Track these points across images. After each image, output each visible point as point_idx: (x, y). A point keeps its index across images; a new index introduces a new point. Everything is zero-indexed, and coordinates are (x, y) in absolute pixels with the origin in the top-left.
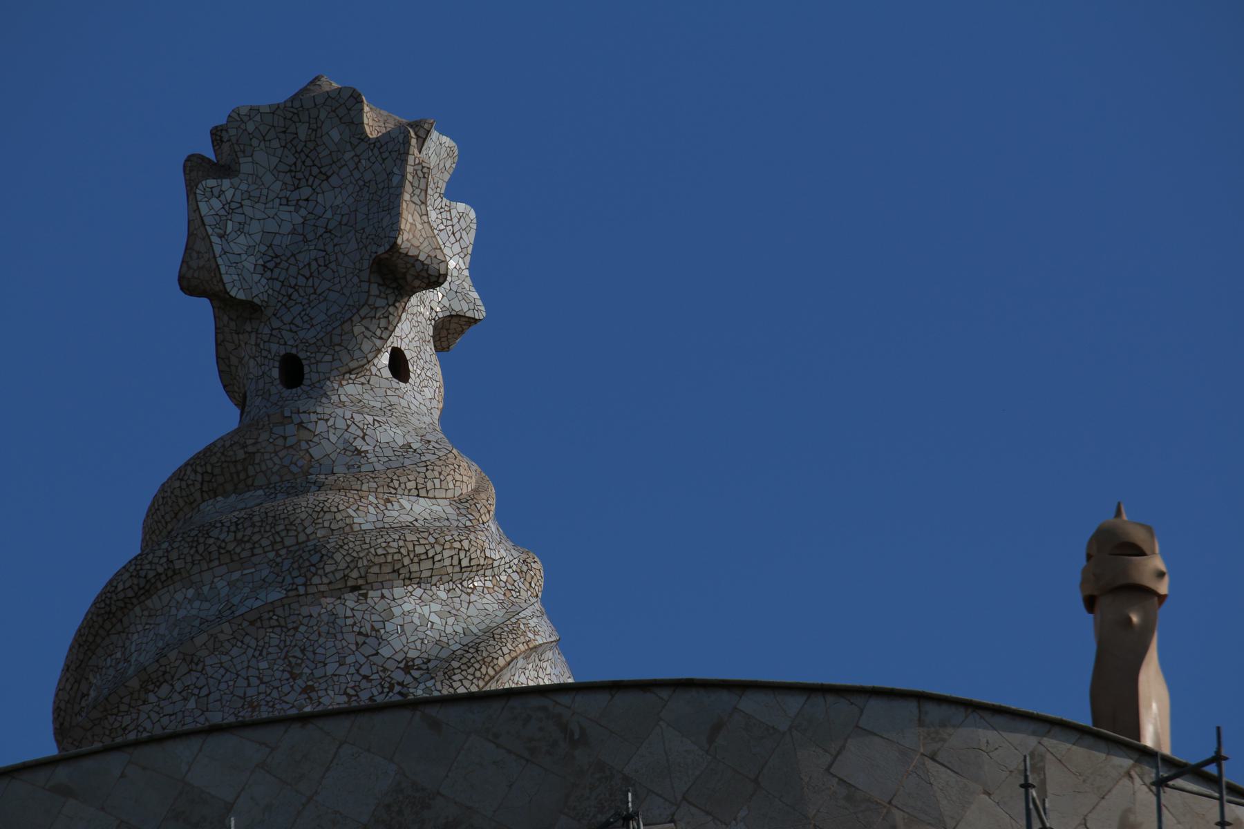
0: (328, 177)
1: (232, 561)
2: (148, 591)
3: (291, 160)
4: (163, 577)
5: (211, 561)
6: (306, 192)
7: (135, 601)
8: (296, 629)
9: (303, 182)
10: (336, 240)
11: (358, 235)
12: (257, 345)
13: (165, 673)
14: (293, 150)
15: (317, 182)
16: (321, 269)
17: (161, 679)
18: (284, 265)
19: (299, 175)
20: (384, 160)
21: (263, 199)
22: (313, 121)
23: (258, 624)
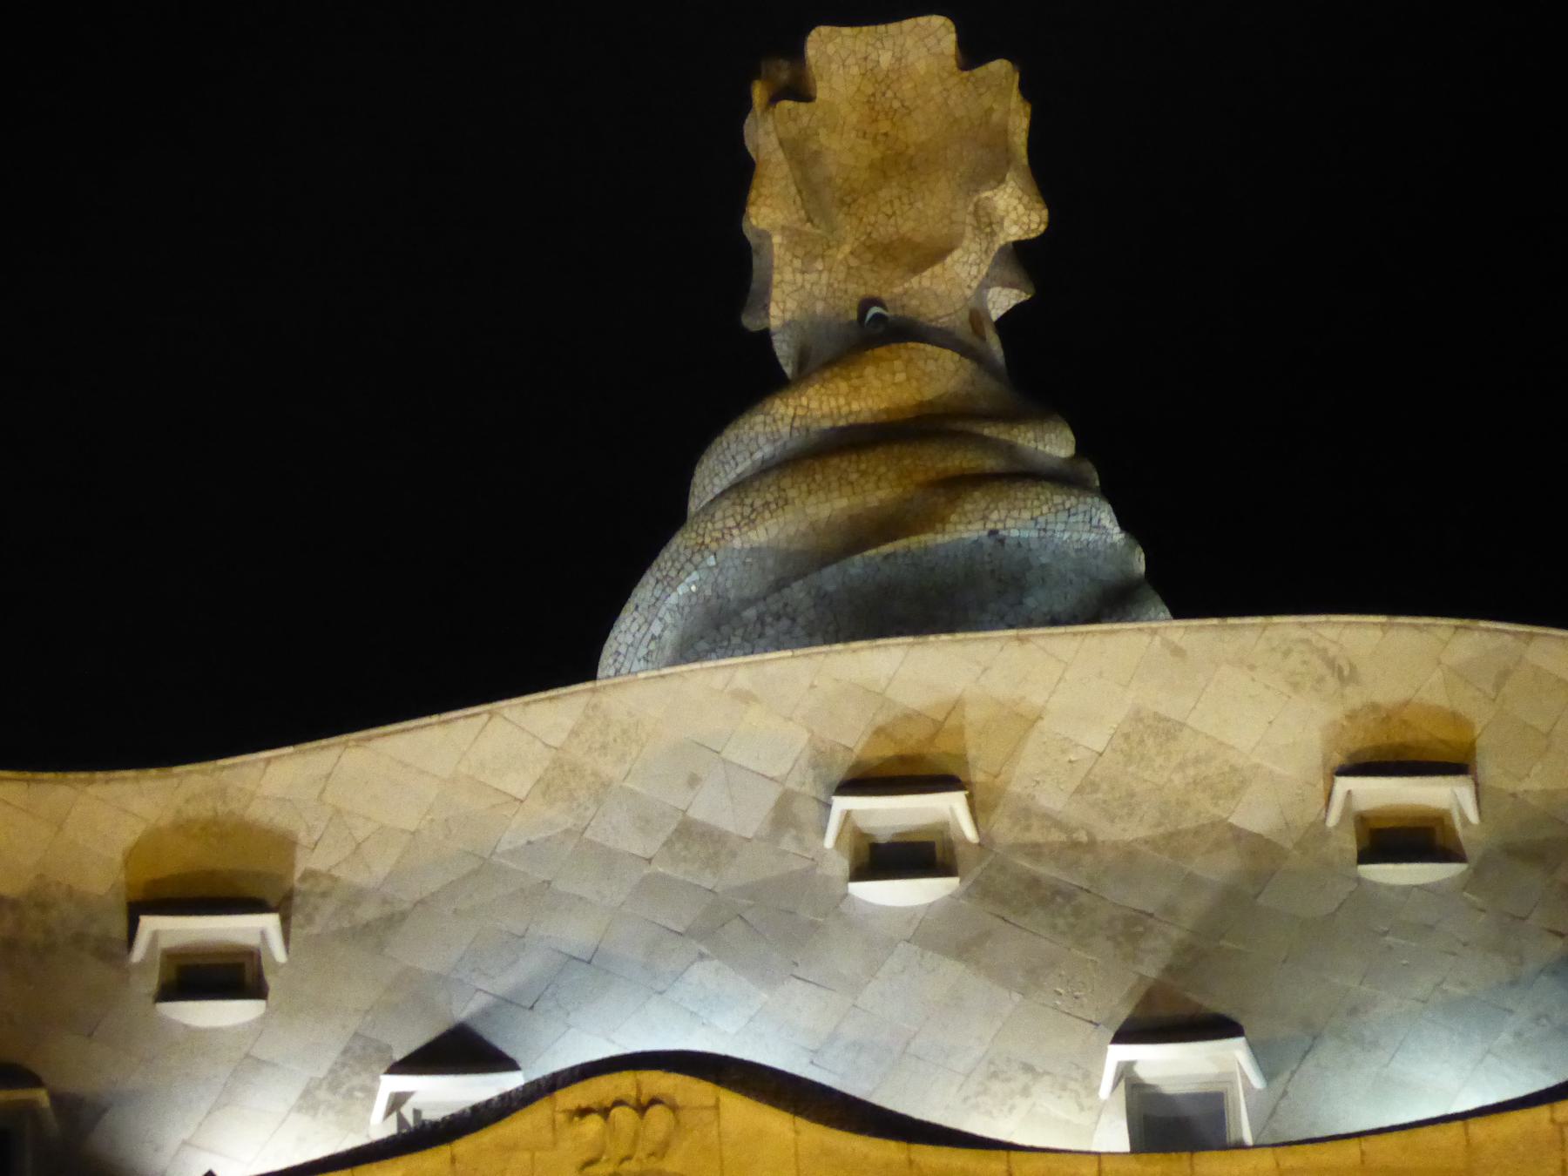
6: (884, 126)
18: (862, 201)
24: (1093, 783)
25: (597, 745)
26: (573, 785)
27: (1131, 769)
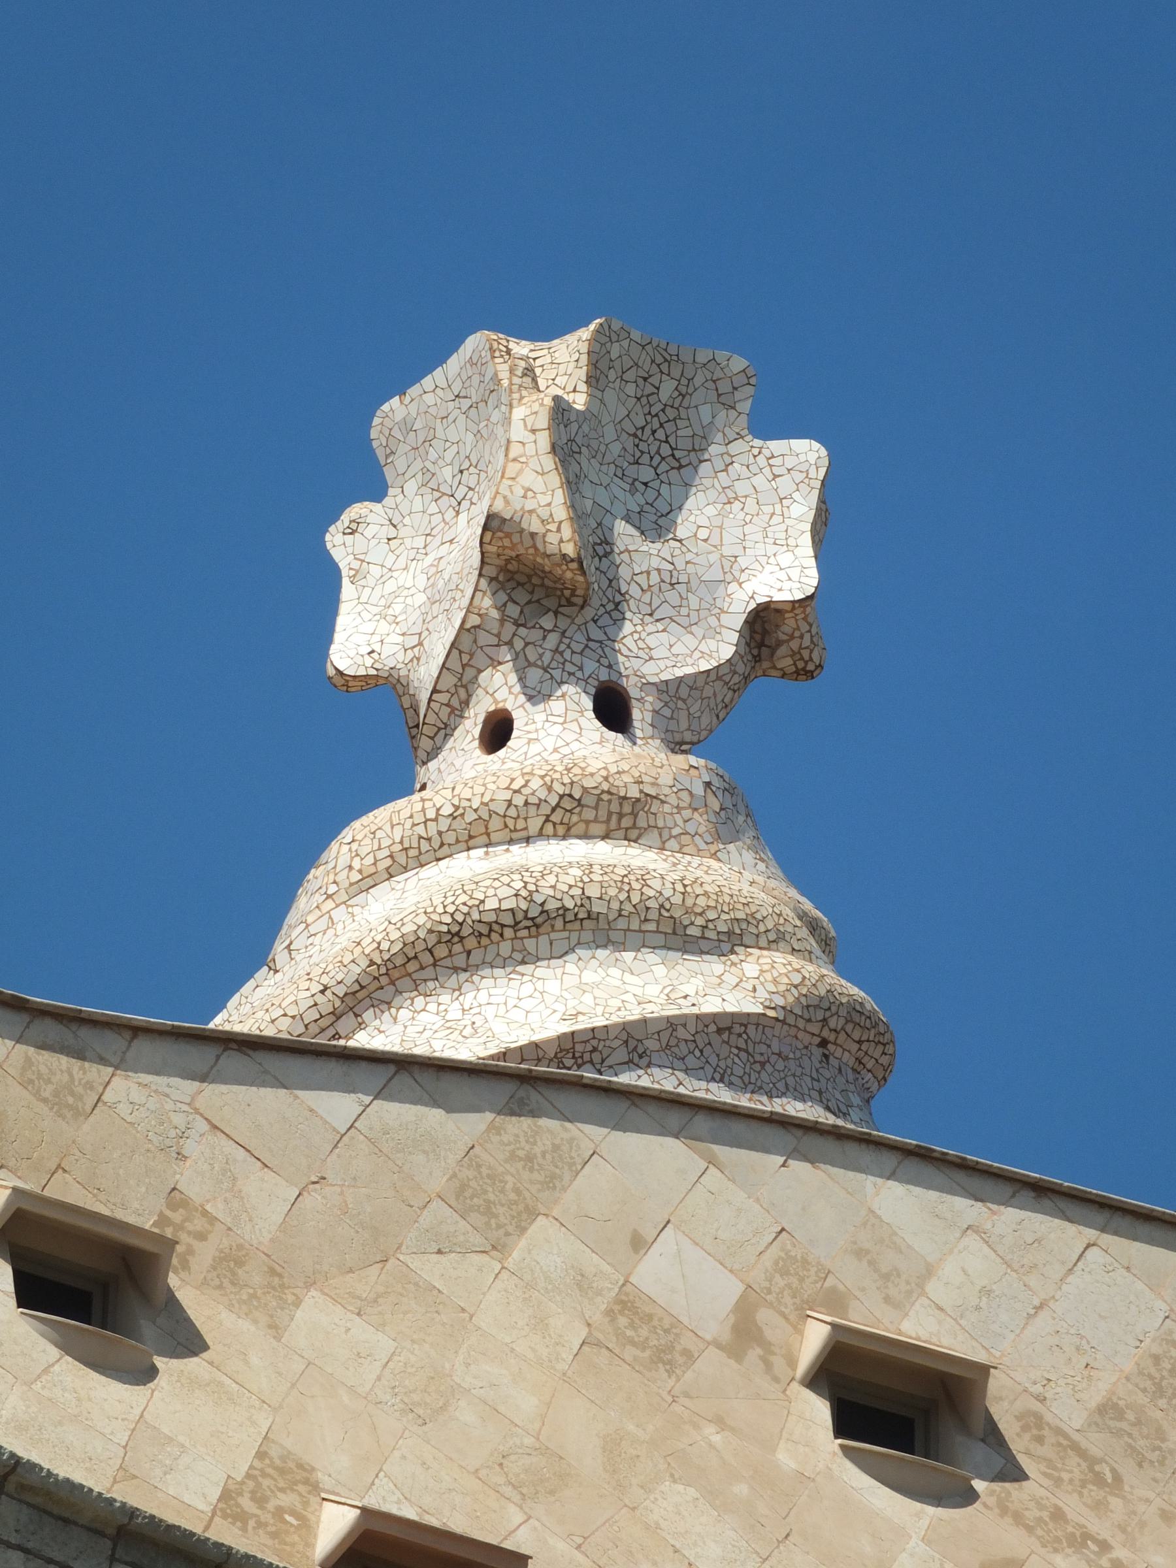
0: (681, 467)
1: (674, 933)
2: (537, 926)
3: (640, 422)
4: (570, 917)
5: (646, 920)
6: (646, 474)
7: (508, 933)
8: (763, 1064)
9: (645, 459)
10: (689, 557)
11: (727, 565)
12: (556, 651)
13: (595, 1049)
14: (646, 410)
15: (664, 467)
16: (665, 587)
17: (587, 1057)
19: (643, 446)
20: (775, 476)
21: (599, 456)
22: (684, 381)
23: (725, 1036)
24: (1115, 1406)
25: (521, 1153)
26: (491, 1197)
27: (1162, 1403)
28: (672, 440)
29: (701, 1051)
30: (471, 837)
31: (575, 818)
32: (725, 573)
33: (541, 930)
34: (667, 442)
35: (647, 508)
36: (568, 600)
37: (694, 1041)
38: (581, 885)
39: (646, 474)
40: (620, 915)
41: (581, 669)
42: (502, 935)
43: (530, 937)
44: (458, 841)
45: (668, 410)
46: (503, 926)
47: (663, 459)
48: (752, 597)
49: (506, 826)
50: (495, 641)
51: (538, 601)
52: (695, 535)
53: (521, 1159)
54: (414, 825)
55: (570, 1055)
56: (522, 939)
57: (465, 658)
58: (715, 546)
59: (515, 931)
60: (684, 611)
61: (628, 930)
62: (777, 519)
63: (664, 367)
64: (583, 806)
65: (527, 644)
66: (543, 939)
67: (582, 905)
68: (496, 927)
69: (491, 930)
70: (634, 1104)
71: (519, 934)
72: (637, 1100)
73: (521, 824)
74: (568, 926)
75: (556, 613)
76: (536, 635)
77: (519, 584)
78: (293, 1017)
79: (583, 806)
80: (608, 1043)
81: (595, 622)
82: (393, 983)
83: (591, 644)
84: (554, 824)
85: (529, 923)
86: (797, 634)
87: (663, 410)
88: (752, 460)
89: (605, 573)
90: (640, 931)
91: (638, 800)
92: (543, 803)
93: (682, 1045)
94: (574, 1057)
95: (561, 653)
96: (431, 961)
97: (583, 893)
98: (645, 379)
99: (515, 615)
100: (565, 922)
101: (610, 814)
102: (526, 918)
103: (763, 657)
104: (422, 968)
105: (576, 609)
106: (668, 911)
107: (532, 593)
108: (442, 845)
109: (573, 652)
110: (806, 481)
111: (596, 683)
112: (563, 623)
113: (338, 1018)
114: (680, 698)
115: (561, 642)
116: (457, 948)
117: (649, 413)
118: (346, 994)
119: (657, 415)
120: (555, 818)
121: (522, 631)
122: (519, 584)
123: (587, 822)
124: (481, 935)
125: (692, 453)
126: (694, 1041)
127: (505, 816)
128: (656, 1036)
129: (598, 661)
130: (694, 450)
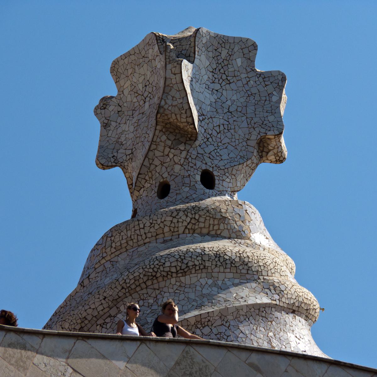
0: (230, 83)
1: (237, 272)
2: (185, 272)
5: (226, 268)
7: (174, 275)
11: (249, 121)
12: (186, 158)
17: (206, 324)
19: (216, 76)
20: (266, 85)
21: (199, 81)
25: (188, 373)
28: (226, 73)
29: (249, 319)
30: (157, 235)
31: (197, 227)
32: (248, 124)
33: (187, 273)
34: (225, 74)
35: (218, 100)
36: (190, 138)
37: (246, 315)
38: (201, 255)
39: (217, 86)
40: (216, 267)
41: (195, 165)
42: (172, 276)
43: (182, 276)
44: (152, 236)
45: (225, 61)
46: (172, 272)
47: (223, 80)
48: (259, 134)
49: (170, 230)
50: (162, 154)
51: (178, 139)
52: (237, 110)
53: (188, 375)
54: (135, 230)
55: (200, 323)
56: (179, 277)
57: (151, 161)
58: (244, 114)
59: (177, 274)
60: (233, 140)
61: (219, 272)
62: (267, 102)
63: (223, 45)
64: (199, 222)
65: (174, 156)
66: (187, 277)
67: (202, 264)
68: (169, 273)
69: (168, 274)
70: (229, 350)
71: (178, 275)
72: (230, 349)
73: (176, 229)
74: (197, 272)
75: (185, 144)
76: (178, 152)
77: (171, 132)
78: (93, 309)
79: (199, 222)
80: (214, 318)
81: (200, 146)
82: (131, 295)
83: (199, 155)
84: (189, 229)
85: (182, 271)
86: (276, 147)
87: (223, 62)
88: (257, 79)
89: (203, 127)
90: (224, 272)
91: (220, 219)
92: (184, 221)
93: (242, 317)
94: (201, 324)
95: (188, 159)
96: (145, 286)
97: (202, 259)
98: (216, 50)
99: (170, 144)
100: (196, 270)
101: (210, 225)
102: (181, 269)
103: (263, 156)
104: (142, 289)
105: (192, 142)
106: (234, 264)
107: (176, 136)
108: (146, 238)
109: (192, 158)
110: (278, 87)
111: (201, 171)
112: (188, 147)
113: (111, 309)
114: (233, 174)
115: (187, 155)
116: (155, 281)
117: (218, 63)
118: (113, 300)
119: (220, 64)
120: (189, 227)
121: (172, 151)
122: (171, 132)
123: (201, 228)
124: (164, 276)
125: (234, 78)
126: (246, 315)
127: (170, 227)
128: (232, 314)
129: (202, 162)
130: (235, 76)
